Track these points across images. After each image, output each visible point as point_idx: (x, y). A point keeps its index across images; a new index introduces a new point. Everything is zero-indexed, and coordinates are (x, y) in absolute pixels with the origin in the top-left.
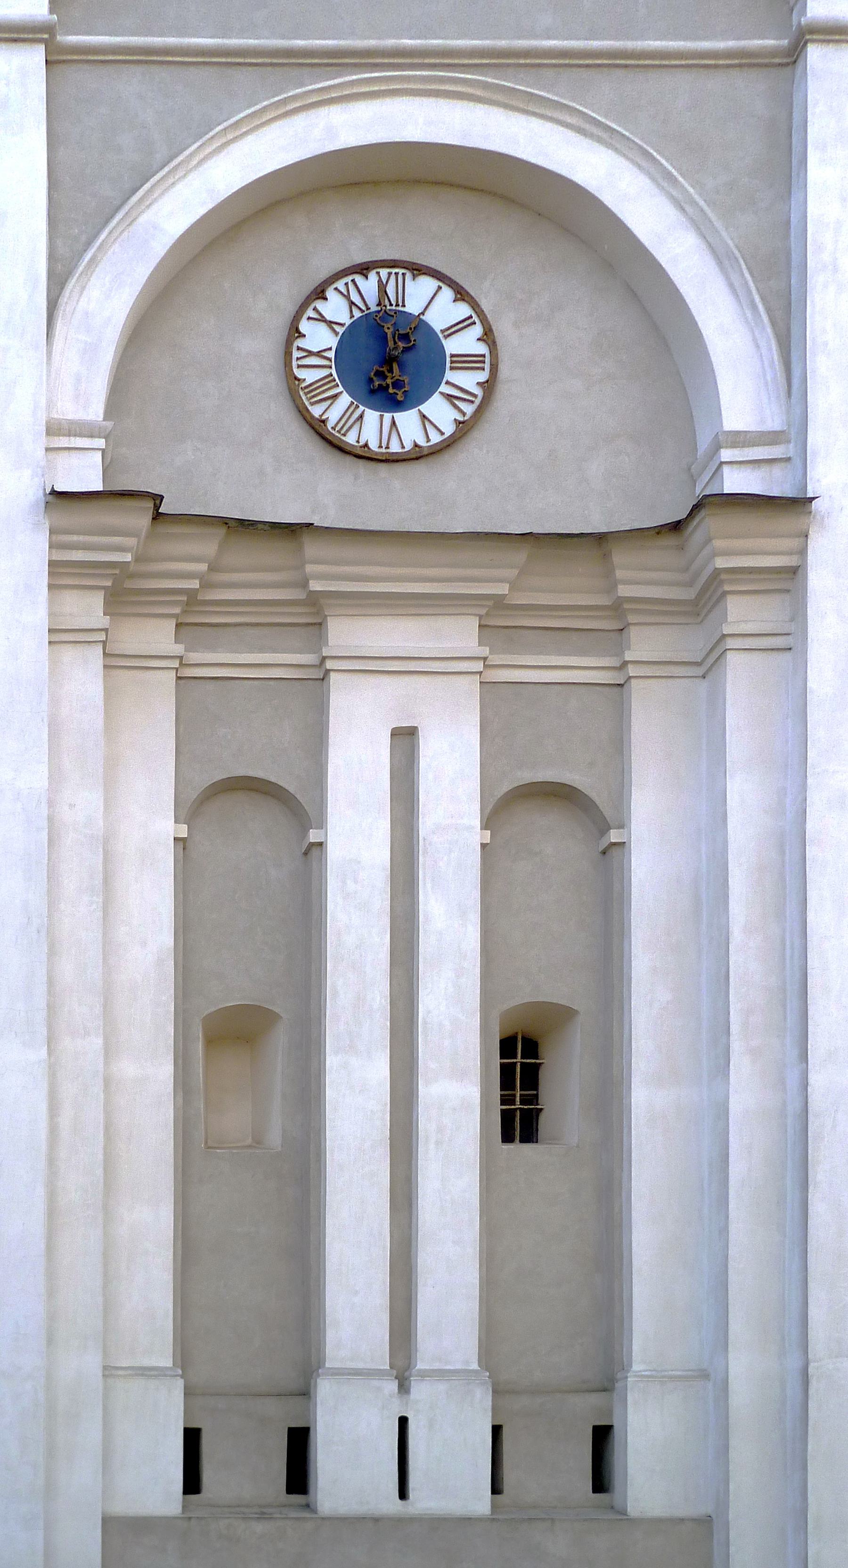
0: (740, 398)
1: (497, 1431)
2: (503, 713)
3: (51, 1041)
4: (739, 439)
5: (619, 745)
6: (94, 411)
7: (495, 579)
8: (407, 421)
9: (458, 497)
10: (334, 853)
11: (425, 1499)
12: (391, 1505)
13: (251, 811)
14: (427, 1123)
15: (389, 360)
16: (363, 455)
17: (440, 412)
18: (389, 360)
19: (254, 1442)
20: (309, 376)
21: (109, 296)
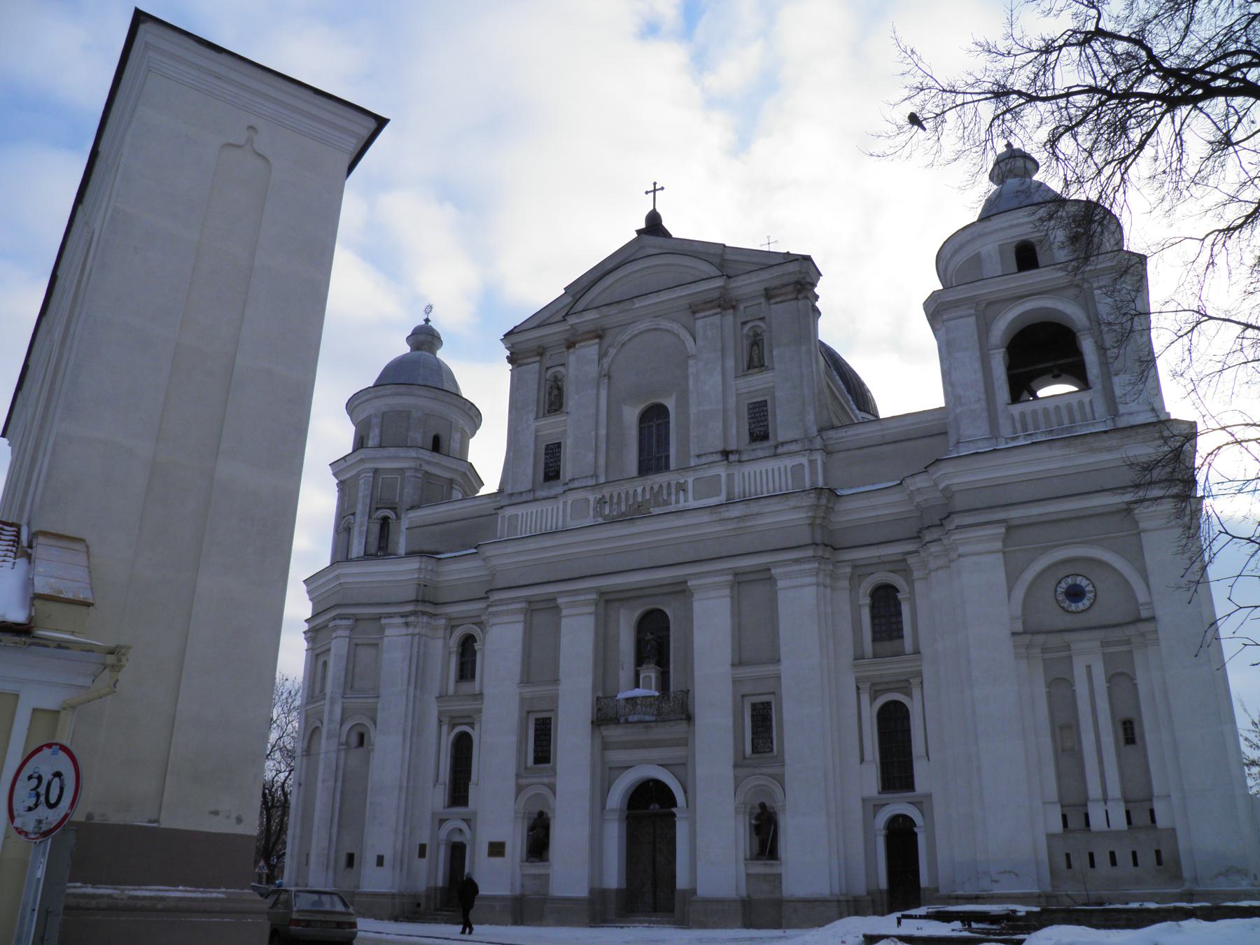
0: (1142, 597)
2: (1108, 660)
4: (1143, 605)
5: (1132, 662)
6: (1019, 612)
7: (1101, 634)
10: (1078, 691)
11: (1114, 827)
14: (1103, 747)
15: (1075, 594)
16: (1072, 612)
18: (1075, 594)
19: (1075, 815)
20: (1060, 598)
21: (1019, 593)
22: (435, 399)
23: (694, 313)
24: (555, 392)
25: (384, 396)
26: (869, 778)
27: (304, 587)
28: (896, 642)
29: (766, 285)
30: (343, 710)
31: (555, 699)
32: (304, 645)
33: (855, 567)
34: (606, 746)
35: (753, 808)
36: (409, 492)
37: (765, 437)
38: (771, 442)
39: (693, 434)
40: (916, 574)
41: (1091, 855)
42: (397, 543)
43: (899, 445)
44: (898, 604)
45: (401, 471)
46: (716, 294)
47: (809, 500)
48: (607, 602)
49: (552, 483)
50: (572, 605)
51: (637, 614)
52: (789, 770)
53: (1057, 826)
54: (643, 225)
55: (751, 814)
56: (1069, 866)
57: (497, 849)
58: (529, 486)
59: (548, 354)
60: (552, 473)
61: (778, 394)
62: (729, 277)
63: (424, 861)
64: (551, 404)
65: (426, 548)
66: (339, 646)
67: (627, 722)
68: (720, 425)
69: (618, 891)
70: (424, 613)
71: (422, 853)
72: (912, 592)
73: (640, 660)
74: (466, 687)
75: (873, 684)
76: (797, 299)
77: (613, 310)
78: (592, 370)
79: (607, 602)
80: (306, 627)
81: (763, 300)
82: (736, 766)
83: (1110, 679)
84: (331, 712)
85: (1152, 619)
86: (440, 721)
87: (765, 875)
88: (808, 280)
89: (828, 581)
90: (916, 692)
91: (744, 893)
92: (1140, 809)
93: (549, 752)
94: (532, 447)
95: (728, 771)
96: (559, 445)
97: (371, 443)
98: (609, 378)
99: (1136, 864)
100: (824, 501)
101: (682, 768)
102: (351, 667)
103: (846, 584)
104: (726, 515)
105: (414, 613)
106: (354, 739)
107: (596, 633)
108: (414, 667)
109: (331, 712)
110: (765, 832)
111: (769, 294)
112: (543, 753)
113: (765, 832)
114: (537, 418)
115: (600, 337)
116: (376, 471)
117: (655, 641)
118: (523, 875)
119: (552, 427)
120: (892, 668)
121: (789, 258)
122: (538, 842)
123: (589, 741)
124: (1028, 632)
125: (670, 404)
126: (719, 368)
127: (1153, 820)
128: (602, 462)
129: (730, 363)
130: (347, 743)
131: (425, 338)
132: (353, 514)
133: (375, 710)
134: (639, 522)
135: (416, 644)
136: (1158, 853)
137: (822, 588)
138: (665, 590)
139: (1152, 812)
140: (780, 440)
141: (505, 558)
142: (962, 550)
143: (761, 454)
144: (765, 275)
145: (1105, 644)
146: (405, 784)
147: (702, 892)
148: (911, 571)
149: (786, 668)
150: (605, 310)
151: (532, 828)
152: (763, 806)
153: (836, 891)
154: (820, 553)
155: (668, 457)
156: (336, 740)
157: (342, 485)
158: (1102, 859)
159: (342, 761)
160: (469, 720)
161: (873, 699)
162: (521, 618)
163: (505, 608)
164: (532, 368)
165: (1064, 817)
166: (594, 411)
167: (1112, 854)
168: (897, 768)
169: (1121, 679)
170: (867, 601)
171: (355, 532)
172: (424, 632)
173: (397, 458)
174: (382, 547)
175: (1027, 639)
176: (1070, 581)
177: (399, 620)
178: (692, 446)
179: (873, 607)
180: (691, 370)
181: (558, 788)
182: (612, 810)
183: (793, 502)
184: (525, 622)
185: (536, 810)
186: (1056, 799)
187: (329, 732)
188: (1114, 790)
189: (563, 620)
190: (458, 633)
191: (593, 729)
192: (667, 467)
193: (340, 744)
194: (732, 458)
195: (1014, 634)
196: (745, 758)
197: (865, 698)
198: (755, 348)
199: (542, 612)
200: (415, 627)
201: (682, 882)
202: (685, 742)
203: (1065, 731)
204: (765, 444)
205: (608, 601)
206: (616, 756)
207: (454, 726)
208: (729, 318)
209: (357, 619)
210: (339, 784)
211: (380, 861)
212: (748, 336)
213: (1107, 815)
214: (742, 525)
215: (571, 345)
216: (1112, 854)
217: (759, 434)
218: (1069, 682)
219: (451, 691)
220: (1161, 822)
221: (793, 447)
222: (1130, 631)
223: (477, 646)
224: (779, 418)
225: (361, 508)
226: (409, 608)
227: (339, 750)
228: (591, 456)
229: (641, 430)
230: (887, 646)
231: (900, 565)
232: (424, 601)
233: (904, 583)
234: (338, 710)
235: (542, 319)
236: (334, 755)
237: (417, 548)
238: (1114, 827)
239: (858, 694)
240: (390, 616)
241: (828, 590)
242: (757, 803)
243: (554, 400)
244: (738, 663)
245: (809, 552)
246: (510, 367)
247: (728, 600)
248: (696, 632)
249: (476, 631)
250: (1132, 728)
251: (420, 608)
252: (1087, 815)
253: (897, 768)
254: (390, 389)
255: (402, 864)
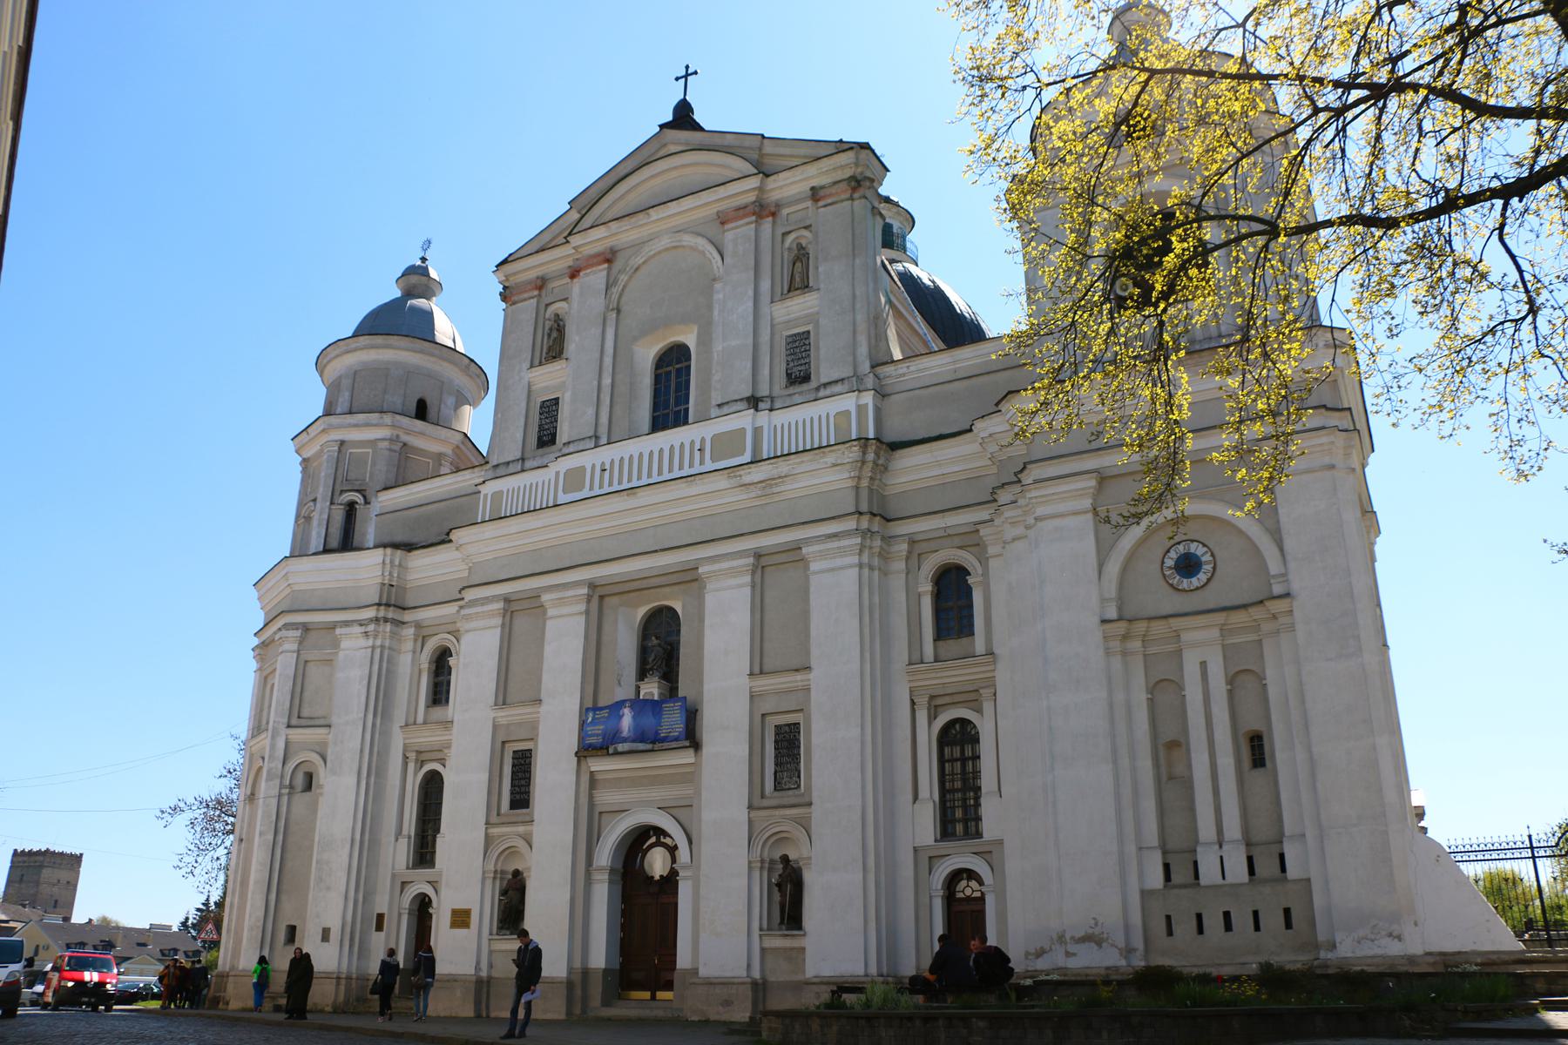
0: (1274, 567)
1: (1250, 860)
2: (1228, 652)
3: (1115, 762)
5: (1262, 656)
7: (1220, 618)
8: (1194, 580)
9: (1210, 598)
11: (1230, 879)
12: (1220, 881)
13: (1164, 689)
15: (1188, 566)
17: (1202, 577)
18: (1188, 566)
19: (1179, 865)
20: (1167, 573)
21: (1113, 568)
22: (421, 352)
23: (723, 223)
24: (555, 334)
25: (356, 350)
26: (922, 823)
27: (254, 593)
28: (965, 641)
29: (815, 182)
30: (287, 743)
31: (534, 726)
32: (254, 665)
33: (912, 542)
34: (593, 782)
35: (772, 862)
36: (380, 470)
37: (806, 378)
38: (813, 384)
39: (716, 377)
40: (991, 550)
41: (1199, 917)
42: (364, 535)
43: (974, 380)
44: (969, 591)
45: (372, 443)
46: (751, 197)
47: (852, 453)
48: (602, 597)
49: (546, 450)
50: (561, 602)
51: (642, 611)
52: (816, 812)
53: (1156, 879)
54: (670, 118)
55: (770, 870)
56: (1170, 933)
57: (461, 919)
58: (518, 455)
59: (551, 285)
60: (547, 439)
61: (823, 322)
62: (767, 176)
63: (382, 935)
64: (549, 349)
65: (399, 538)
66: (285, 663)
67: (617, 753)
68: (749, 365)
69: (605, 971)
70: (386, 620)
71: (379, 928)
72: (986, 574)
73: (642, 674)
74: (437, 712)
75: (932, 697)
76: (852, 199)
77: (625, 224)
78: (598, 303)
79: (602, 597)
80: (256, 641)
81: (809, 203)
82: (750, 807)
83: (1231, 681)
84: (273, 747)
85: (1287, 595)
86: (406, 758)
87: (785, 950)
88: (868, 174)
89: (876, 562)
90: (988, 707)
91: (757, 975)
92: (1266, 856)
93: (528, 793)
94: (524, 404)
95: (739, 814)
96: (557, 399)
97: (339, 410)
98: (619, 311)
99: (1257, 928)
100: (871, 456)
101: (682, 810)
102: (298, 689)
103: (902, 565)
104: (747, 479)
105: (377, 619)
106: (300, 780)
107: (586, 638)
108: (373, 691)
109: (273, 747)
110: (786, 895)
111: (815, 194)
112: (521, 799)
113: (786, 895)
114: (532, 366)
115: (608, 261)
116: (342, 443)
117: (662, 644)
118: (491, 952)
119: (549, 379)
120: (955, 676)
121: (842, 147)
122: (511, 913)
123: (574, 778)
124: (1123, 621)
125: (690, 340)
126: (751, 293)
127: (1283, 869)
128: (604, 419)
129: (765, 285)
130: (291, 787)
131: (417, 281)
132: (315, 500)
133: (325, 744)
134: (641, 492)
135: (377, 657)
136: (1287, 912)
137: (866, 571)
138: (674, 579)
139: (1282, 856)
140: (824, 380)
141: (478, 545)
142: (1040, 511)
143: (797, 399)
144: (812, 170)
145: (1224, 631)
146: (358, 837)
147: (703, 972)
148: (985, 548)
149: (816, 677)
150: (614, 225)
151: (504, 893)
152: (785, 859)
153: (873, 970)
154: (865, 524)
155: (687, 410)
156: (277, 782)
157: (305, 462)
158: (1214, 923)
159: (284, 809)
160: (439, 756)
161: (932, 717)
162: (499, 621)
163: (479, 609)
164: (528, 307)
165: (1167, 867)
166: (597, 355)
167: (1227, 915)
168: (959, 809)
169: (1244, 678)
170: (926, 588)
171: (315, 523)
172: (387, 644)
173: (367, 425)
174: (346, 541)
175: (1121, 627)
176: (1181, 547)
177: (358, 629)
178: (713, 394)
179: (938, 596)
180: (718, 296)
181: (535, 841)
182: (601, 869)
183: (830, 458)
184: (503, 625)
185: (511, 868)
186: (1155, 843)
187: (269, 772)
188: (1233, 829)
189: (549, 623)
190: (432, 644)
191: (579, 762)
192: (686, 423)
193: (282, 786)
194: (761, 405)
195: (1104, 621)
196: (763, 796)
197: (922, 716)
198: (798, 265)
199: (521, 615)
200: (375, 637)
201: (683, 960)
202: (690, 777)
203: (1170, 750)
204: (805, 387)
205: (600, 597)
206: (606, 798)
207: (423, 763)
208: (767, 224)
209: (306, 628)
210: (280, 837)
211: (326, 935)
212: (790, 249)
213: (1224, 864)
214: (768, 491)
215: (574, 274)
216: (1227, 915)
217: (799, 377)
218: (1180, 687)
219: (420, 719)
220: (1293, 871)
221: (838, 388)
222: (1256, 613)
223: (452, 661)
224: (822, 352)
225: (323, 492)
226: (370, 613)
227: (280, 795)
228: (591, 411)
229: (657, 379)
230: (952, 646)
231: (971, 539)
232: (388, 605)
233: (977, 564)
234: (281, 745)
235: (541, 244)
236: (274, 802)
237: (387, 540)
238: (1230, 879)
239: (913, 711)
240: (347, 624)
241: (876, 573)
242: (777, 855)
243: (553, 345)
244: (759, 669)
245: (850, 524)
246: (504, 305)
247: (748, 590)
248: (708, 632)
249: (448, 640)
250: (1261, 746)
251: (381, 614)
252: (1196, 863)
253: (959, 809)
254: (364, 340)
255: (352, 939)
